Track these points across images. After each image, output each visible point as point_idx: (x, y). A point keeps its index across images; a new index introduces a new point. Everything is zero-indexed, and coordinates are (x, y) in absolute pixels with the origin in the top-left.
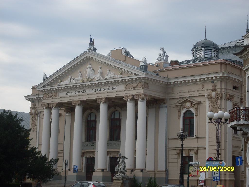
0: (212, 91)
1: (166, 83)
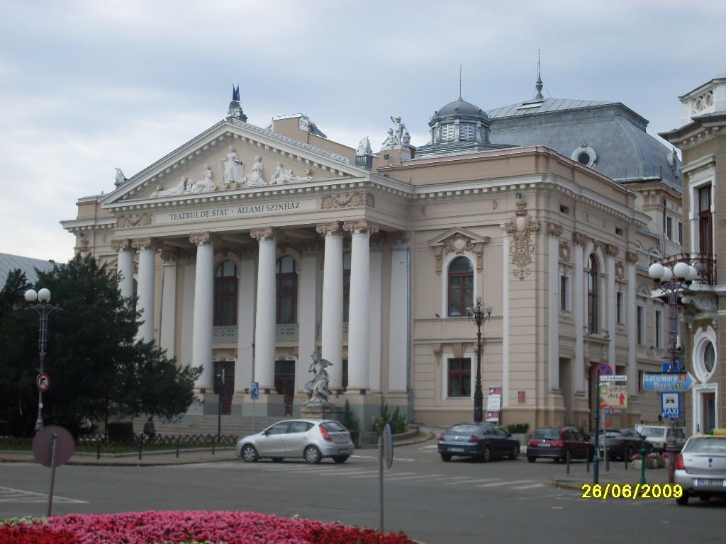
0: (518, 215)
1: (410, 197)
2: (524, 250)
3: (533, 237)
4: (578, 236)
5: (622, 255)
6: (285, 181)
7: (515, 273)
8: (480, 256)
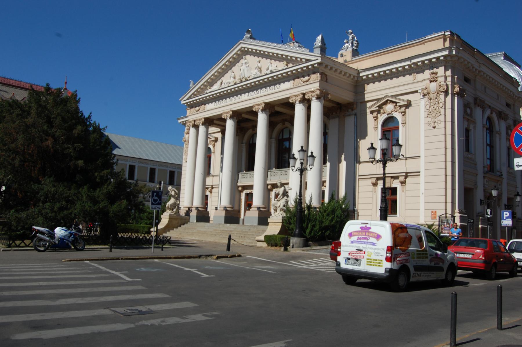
0: (431, 81)
2: (435, 106)
3: (442, 96)
4: (478, 101)
5: (510, 122)
6: (271, 71)
7: (429, 124)
8: (404, 114)
